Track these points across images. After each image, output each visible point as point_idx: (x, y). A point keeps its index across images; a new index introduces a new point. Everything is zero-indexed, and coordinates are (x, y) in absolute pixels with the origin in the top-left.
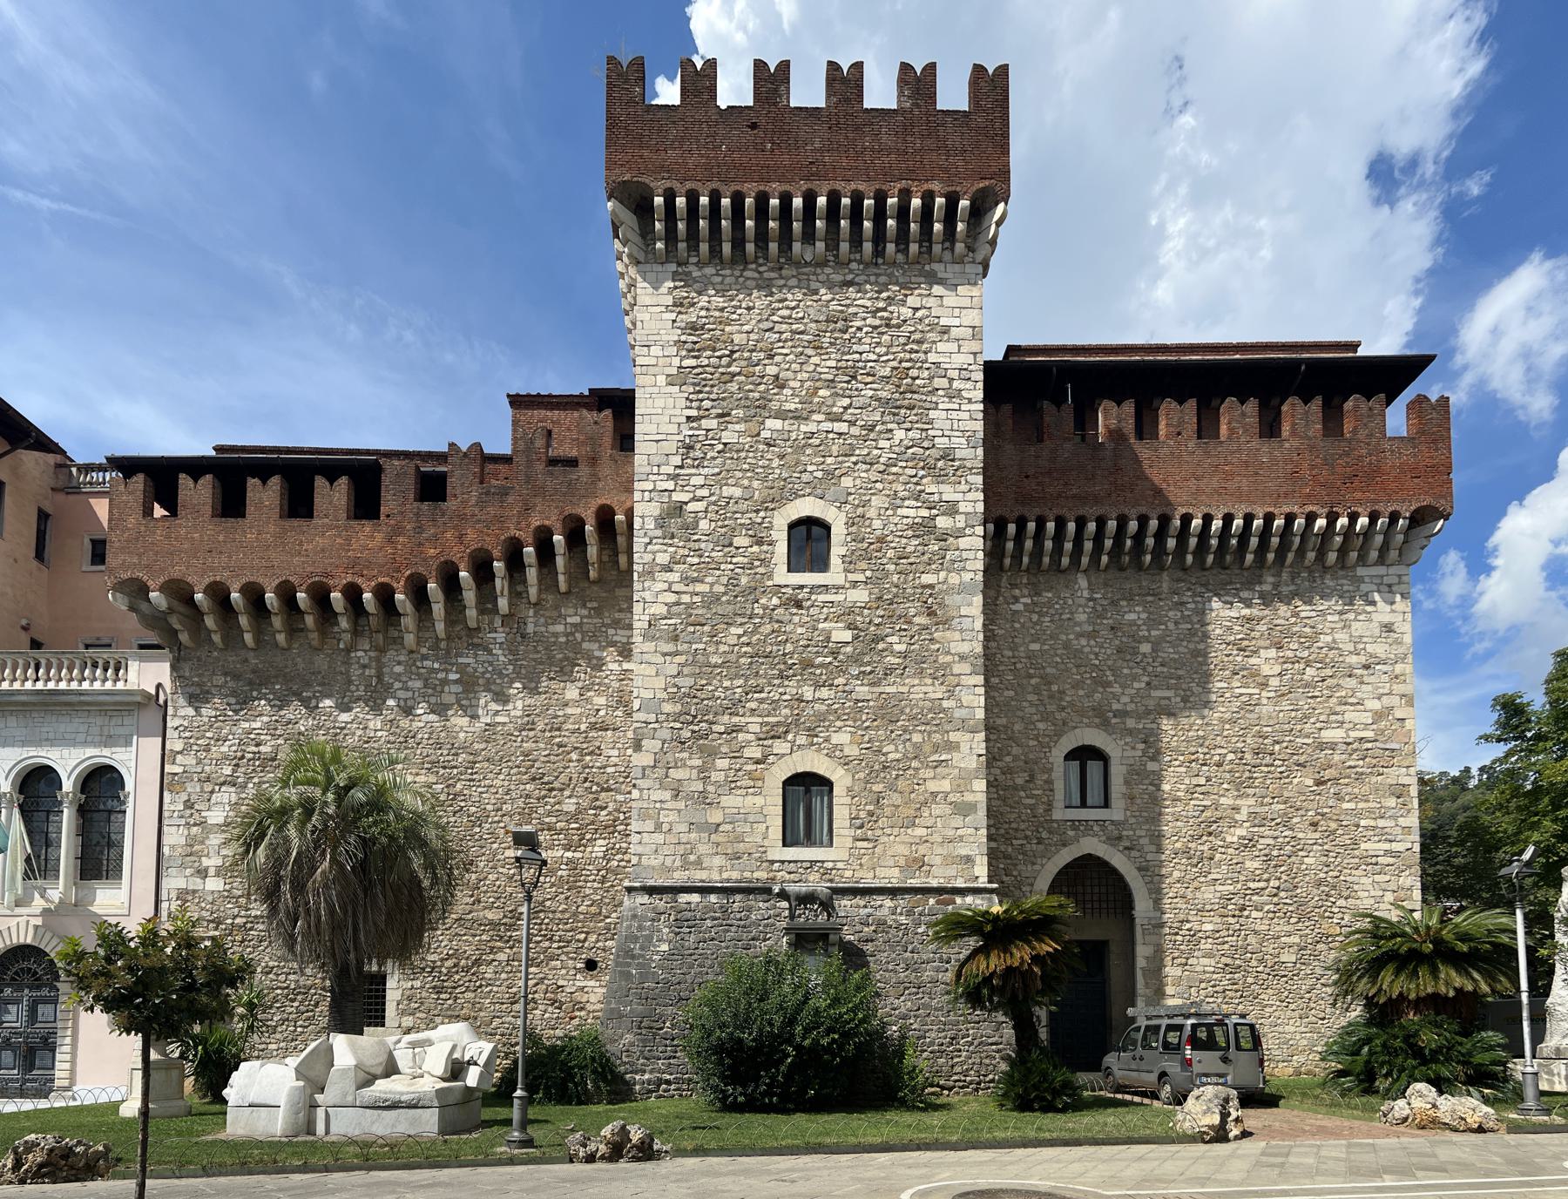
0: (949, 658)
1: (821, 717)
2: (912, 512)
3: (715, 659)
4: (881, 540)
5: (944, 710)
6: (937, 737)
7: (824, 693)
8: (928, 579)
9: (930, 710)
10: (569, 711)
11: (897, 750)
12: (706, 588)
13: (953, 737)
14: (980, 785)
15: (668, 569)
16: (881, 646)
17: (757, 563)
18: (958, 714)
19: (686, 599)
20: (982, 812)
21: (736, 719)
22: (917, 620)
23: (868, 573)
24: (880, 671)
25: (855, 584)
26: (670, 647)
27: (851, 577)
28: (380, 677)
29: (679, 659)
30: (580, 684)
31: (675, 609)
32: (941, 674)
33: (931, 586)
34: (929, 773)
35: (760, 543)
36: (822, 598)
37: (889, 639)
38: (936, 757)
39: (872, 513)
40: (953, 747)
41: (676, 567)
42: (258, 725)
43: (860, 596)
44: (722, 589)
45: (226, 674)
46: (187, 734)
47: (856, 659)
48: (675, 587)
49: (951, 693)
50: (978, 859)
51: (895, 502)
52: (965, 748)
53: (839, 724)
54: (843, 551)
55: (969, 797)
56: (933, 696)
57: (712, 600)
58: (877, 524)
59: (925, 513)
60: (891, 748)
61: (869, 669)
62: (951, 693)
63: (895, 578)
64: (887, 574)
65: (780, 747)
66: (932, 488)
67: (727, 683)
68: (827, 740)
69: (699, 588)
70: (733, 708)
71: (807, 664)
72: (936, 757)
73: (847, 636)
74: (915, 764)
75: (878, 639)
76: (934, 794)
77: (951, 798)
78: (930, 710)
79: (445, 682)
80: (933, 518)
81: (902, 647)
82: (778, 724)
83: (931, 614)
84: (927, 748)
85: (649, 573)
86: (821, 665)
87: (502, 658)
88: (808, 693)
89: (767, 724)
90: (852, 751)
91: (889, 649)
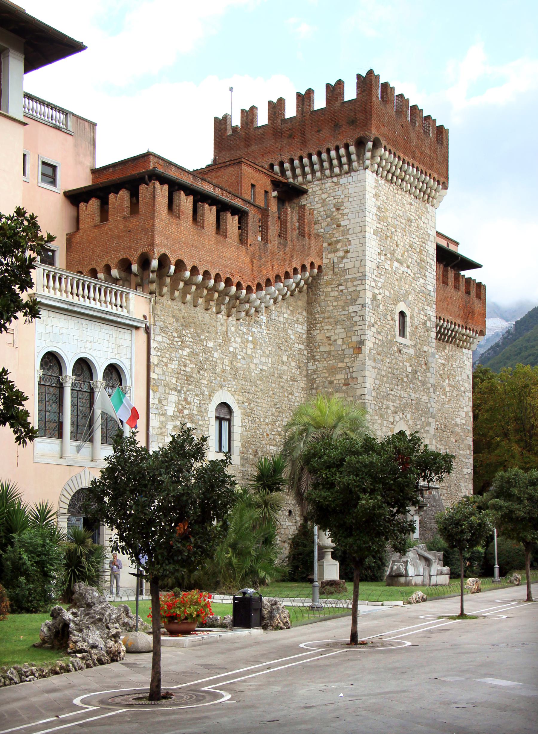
3: (384, 373)
8: (426, 349)
21: (388, 403)
28: (227, 332)
29: (376, 370)
31: (376, 346)
33: (425, 352)
36: (406, 351)
42: (185, 353)
43: (412, 352)
45: (173, 317)
46: (159, 354)
47: (411, 382)
48: (376, 336)
59: (425, 318)
62: (429, 402)
66: (426, 307)
79: (247, 341)
82: (397, 407)
83: (426, 364)
87: (265, 332)
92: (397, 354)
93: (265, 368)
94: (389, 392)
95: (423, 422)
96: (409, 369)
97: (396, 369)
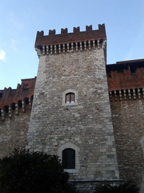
0: (103, 119)
1: (72, 134)
2: (92, 90)
3: (48, 122)
4: (86, 96)
5: (103, 131)
6: (102, 138)
7: (74, 129)
8: (96, 102)
9: (99, 131)
10: (21, 137)
11: (91, 141)
12: (47, 108)
13: (106, 137)
14: (114, 149)
15: (39, 105)
16: (87, 117)
17: (59, 102)
18: (106, 131)
19: (43, 110)
20: (116, 157)
21: (52, 136)
22: (94, 111)
23: (83, 102)
24: (86, 123)
25: (80, 105)
26: (38, 121)
27: (79, 103)
30: (24, 131)
32: (102, 122)
33: (97, 104)
34: (100, 147)
35: (59, 98)
36: (72, 108)
37: (88, 116)
38: (102, 143)
39: (83, 91)
40: (106, 140)
41: (41, 104)
43: (82, 107)
44: (51, 108)
47: (81, 120)
49: (104, 127)
50: (116, 171)
51: (88, 88)
52: (109, 140)
53: (77, 136)
54: (77, 98)
55: (112, 153)
56: (100, 127)
57: (48, 110)
58: (85, 93)
60: (90, 141)
61: (84, 122)
63: (89, 103)
64: (87, 102)
65: (62, 142)
66: (96, 85)
67: (50, 128)
68: (74, 140)
69: (46, 108)
70: (51, 133)
71: (69, 122)
72: (102, 143)
73: (79, 115)
74: (96, 145)
75: (86, 115)
76: (102, 153)
77: (107, 153)
78: (99, 131)
80: (97, 91)
81: (92, 117)
82: (62, 136)
83: (98, 109)
84: (99, 140)
85: (35, 106)
86: (72, 122)
88: (69, 129)
89: (59, 136)
90: (80, 142)
91: (89, 118)
92: (64, 111)
93: (5, 140)
94: (54, 130)
95: (96, 140)
96: (77, 115)
97: (62, 118)
